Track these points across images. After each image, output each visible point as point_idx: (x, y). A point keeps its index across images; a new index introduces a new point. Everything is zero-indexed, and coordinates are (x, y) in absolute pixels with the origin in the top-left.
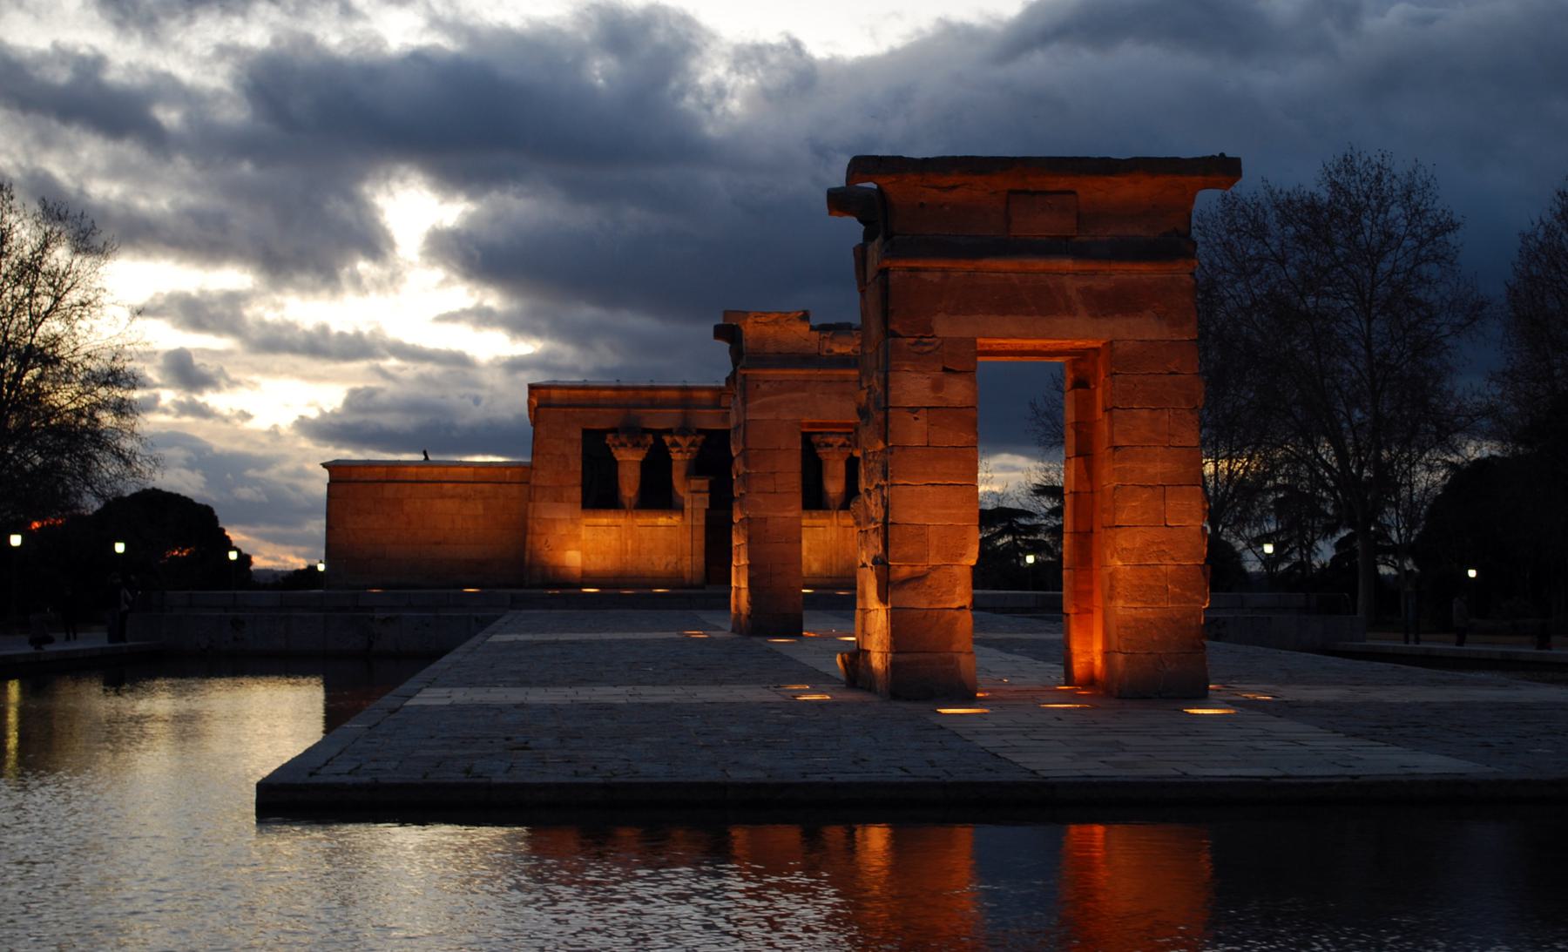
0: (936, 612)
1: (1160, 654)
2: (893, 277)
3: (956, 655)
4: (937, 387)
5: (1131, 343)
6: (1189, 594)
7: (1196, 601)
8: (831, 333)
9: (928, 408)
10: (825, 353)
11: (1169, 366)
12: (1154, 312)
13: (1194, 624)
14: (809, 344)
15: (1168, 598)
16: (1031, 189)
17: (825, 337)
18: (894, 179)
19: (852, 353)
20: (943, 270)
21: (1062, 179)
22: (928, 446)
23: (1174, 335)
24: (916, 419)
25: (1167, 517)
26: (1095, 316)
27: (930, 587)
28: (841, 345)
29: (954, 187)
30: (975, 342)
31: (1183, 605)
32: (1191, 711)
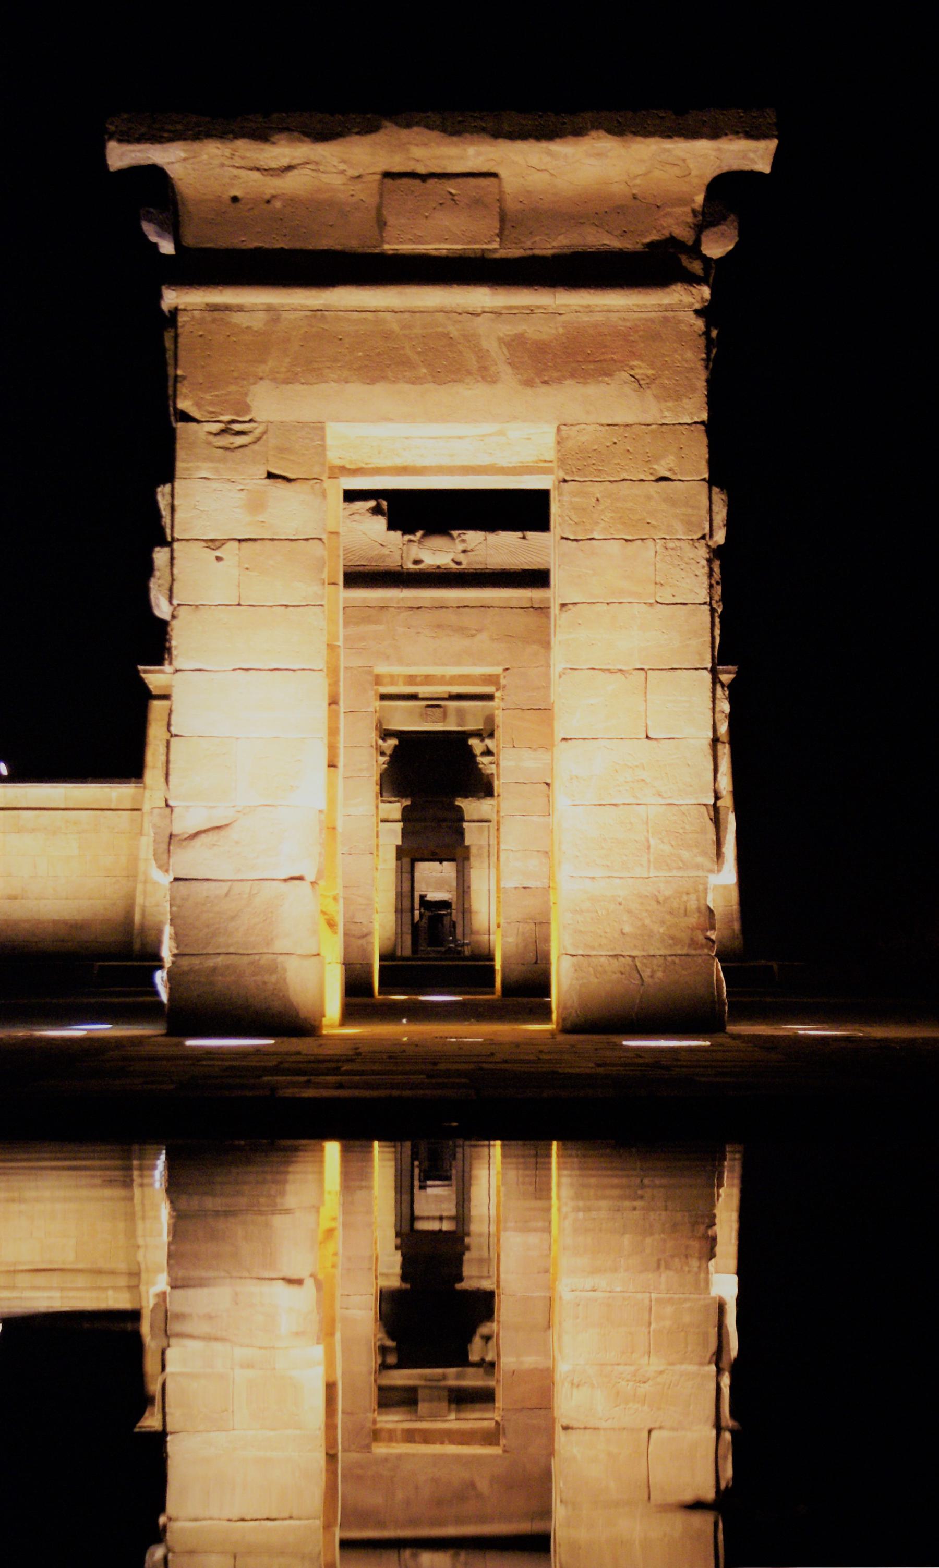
0: (246, 886)
1: (633, 958)
2: (182, 319)
3: (280, 959)
4: (256, 505)
5: (590, 428)
6: (686, 855)
7: (698, 867)
8: (419, 534)
9: (240, 541)
10: (411, 566)
11: (655, 466)
12: (632, 376)
13: (693, 905)
14: (385, 551)
15: (649, 861)
16: (421, 169)
17: (410, 541)
18: (183, 155)
19: (454, 566)
20: (269, 309)
21: (471, 150)
22: (239, 605)
23: (666, 414)
24: (219, 559)
25: (649, 723)
26: (529, 383)
27: (237, 842)
28: (434, 551)
29: (290, 168)
30: (322, 429)
31: (675, 873)
32: (625, 1043)
